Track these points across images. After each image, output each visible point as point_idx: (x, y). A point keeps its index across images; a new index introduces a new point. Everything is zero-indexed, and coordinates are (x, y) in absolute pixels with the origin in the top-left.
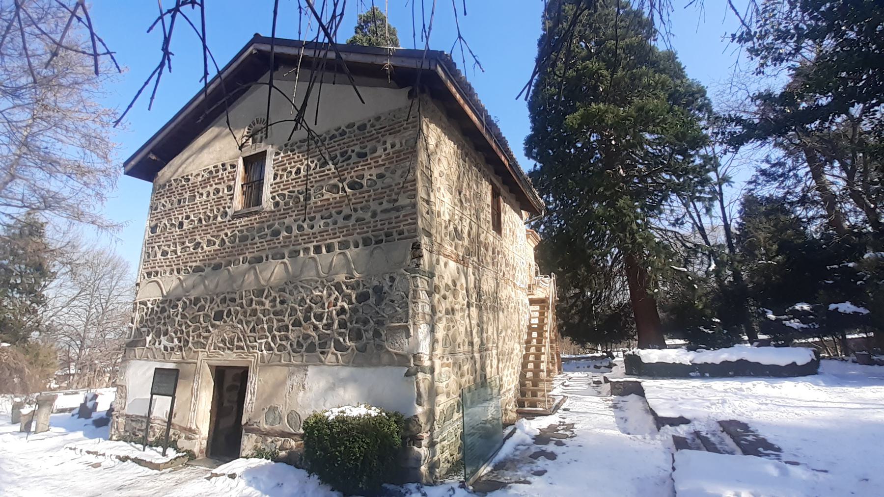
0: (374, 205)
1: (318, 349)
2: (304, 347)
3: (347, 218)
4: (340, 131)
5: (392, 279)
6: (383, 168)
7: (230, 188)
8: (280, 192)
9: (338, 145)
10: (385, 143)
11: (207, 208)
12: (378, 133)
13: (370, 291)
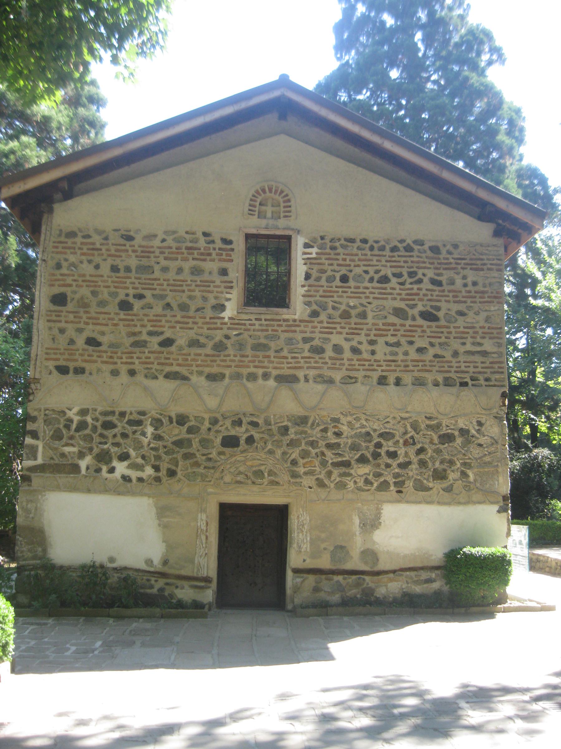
0: (455, 345)
1: (392, 488)
2: (375, 485)
3: (420, 350)
4: (405, 244)
5: (480, 424)
6: (464, 305)
7: (224, 272)
8: (318, 298)
9: (405, 262)
10: (464, 277)
11: (183, 291)
12: (457, 264)
13: (456, 433)
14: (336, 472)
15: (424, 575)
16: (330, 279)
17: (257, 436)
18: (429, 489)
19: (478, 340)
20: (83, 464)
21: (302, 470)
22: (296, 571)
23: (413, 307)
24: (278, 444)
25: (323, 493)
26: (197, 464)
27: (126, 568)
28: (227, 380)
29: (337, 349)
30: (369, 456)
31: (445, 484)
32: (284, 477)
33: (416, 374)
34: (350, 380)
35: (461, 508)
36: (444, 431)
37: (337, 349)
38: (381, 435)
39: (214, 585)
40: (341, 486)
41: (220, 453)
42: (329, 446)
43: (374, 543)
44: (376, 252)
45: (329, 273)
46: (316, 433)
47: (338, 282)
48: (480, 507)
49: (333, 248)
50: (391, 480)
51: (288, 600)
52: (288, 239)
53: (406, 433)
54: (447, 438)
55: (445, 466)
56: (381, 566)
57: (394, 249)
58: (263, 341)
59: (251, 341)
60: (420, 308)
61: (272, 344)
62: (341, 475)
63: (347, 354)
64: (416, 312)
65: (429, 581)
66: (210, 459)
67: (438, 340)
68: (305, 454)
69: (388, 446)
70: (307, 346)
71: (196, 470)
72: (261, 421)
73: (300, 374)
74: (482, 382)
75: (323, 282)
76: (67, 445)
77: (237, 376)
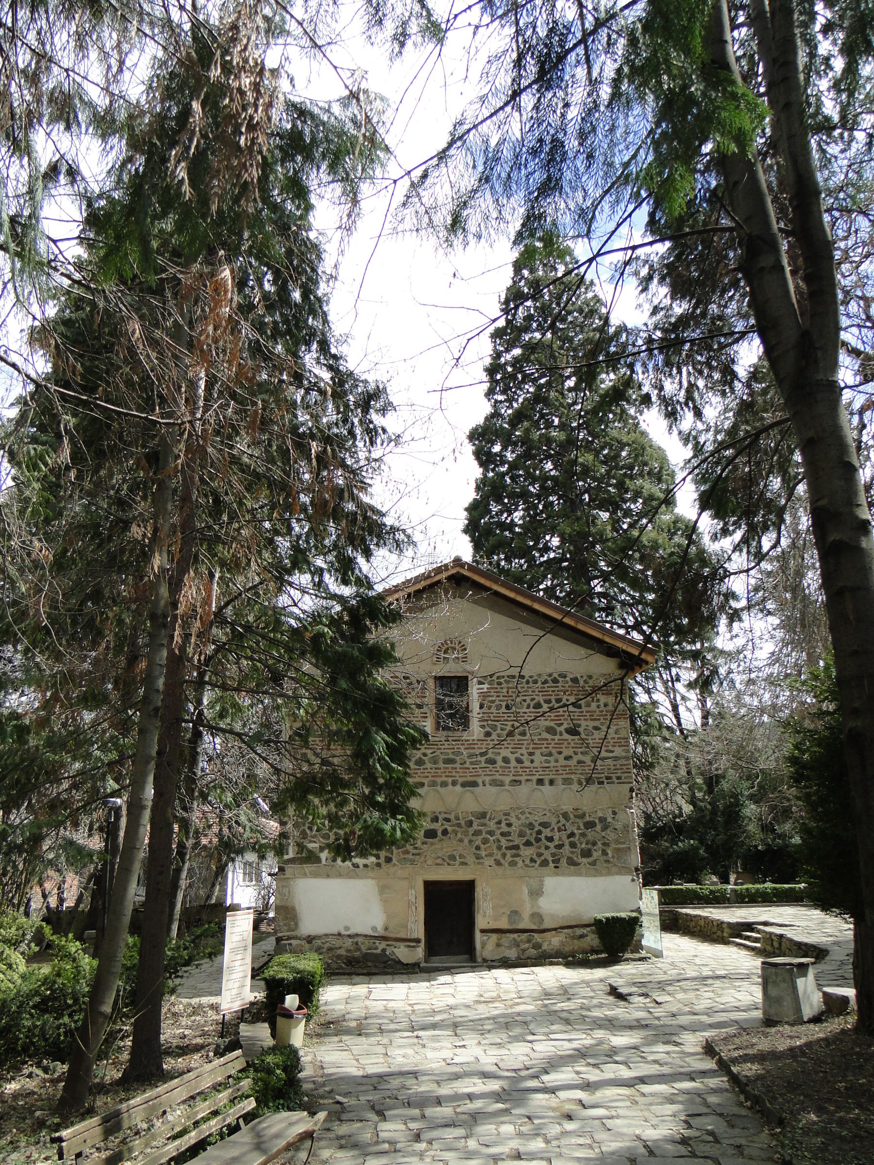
3: (567, 758)
5: (614, 813)
10: (598, 701)
14: (509, 853)
15: (579, 932)
16: (499, 707)
17: (449, 829)
18: (576, 864)
19: (611, 748)
20: (324, 855)
21: (483, 853)
22: (483, 931)
23: (560, 725)
24: (466, 834)
25: (499, 870)
26: (407, 852)
27: (357, 935)
28: (426, 787)
29: (506, 760)
30: (533, 840)
31: (590, 860)
32: (471, 859)
33: (565, 776)
34: (516, 782)
35: (602, 878)
36: (587, 819)
37: (506, 760)
38: (540, 824)
39: (422, 944)
40: (513, 864)
41: (423, 843)
42: (502, 834)
43: (539, 907)
44: (531, 685)
45: (497, 703)
46: (492, 825)
47: (503, 710)
48: (617, 877)
49: (499, 684)
50: (550, 859)
51: (478, 953)
52: (467, 678)
53: (559, 822)
54: (590, 825)
55: (590, 846)
56: (547, 925)
57: (546, 682)
58: (451, 756)
59: (443, 757)
60: (565, 726)
61: (458, 758)
62: (513, 856)
63: (513, 763)
64: (562, 728)
65: (582, 936)
66: (416, 848)
67: (580, 750)
68: (485, 841)
69: (547, 832)
70: (483, 759)
71: (406, 856)
72: (452, 817)
73: (480, 781)
74: (615, 779)
75: (493, 710)
76: (311, 842)
77: (433, 784)
